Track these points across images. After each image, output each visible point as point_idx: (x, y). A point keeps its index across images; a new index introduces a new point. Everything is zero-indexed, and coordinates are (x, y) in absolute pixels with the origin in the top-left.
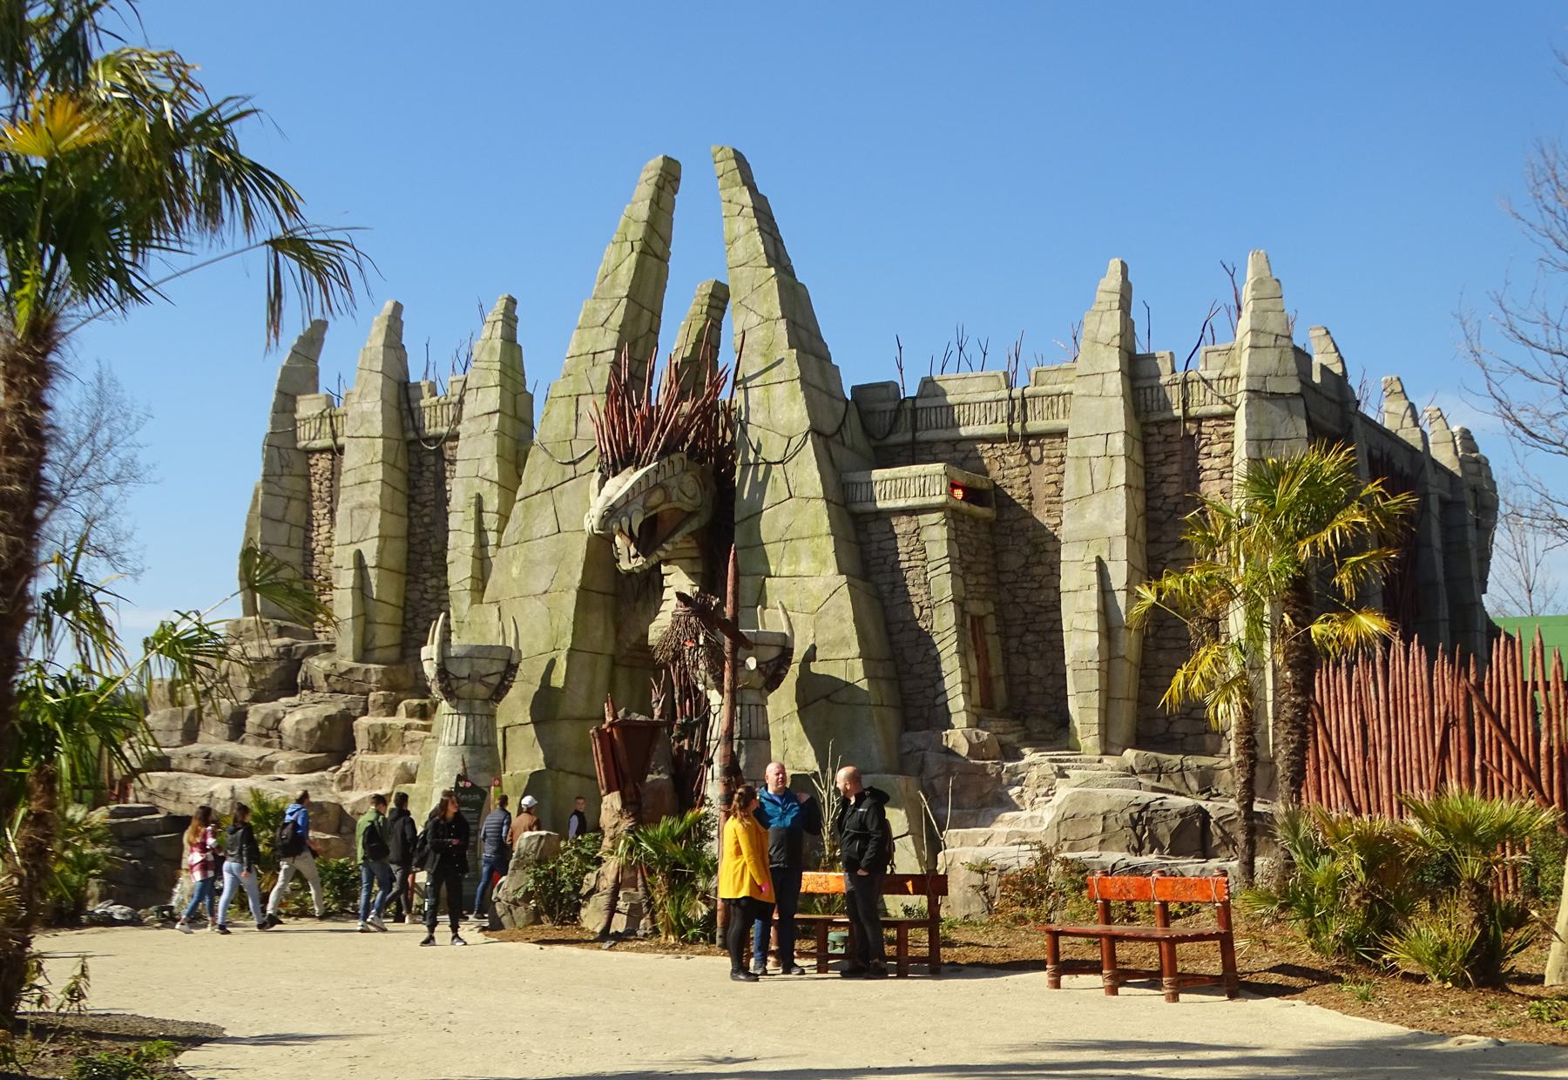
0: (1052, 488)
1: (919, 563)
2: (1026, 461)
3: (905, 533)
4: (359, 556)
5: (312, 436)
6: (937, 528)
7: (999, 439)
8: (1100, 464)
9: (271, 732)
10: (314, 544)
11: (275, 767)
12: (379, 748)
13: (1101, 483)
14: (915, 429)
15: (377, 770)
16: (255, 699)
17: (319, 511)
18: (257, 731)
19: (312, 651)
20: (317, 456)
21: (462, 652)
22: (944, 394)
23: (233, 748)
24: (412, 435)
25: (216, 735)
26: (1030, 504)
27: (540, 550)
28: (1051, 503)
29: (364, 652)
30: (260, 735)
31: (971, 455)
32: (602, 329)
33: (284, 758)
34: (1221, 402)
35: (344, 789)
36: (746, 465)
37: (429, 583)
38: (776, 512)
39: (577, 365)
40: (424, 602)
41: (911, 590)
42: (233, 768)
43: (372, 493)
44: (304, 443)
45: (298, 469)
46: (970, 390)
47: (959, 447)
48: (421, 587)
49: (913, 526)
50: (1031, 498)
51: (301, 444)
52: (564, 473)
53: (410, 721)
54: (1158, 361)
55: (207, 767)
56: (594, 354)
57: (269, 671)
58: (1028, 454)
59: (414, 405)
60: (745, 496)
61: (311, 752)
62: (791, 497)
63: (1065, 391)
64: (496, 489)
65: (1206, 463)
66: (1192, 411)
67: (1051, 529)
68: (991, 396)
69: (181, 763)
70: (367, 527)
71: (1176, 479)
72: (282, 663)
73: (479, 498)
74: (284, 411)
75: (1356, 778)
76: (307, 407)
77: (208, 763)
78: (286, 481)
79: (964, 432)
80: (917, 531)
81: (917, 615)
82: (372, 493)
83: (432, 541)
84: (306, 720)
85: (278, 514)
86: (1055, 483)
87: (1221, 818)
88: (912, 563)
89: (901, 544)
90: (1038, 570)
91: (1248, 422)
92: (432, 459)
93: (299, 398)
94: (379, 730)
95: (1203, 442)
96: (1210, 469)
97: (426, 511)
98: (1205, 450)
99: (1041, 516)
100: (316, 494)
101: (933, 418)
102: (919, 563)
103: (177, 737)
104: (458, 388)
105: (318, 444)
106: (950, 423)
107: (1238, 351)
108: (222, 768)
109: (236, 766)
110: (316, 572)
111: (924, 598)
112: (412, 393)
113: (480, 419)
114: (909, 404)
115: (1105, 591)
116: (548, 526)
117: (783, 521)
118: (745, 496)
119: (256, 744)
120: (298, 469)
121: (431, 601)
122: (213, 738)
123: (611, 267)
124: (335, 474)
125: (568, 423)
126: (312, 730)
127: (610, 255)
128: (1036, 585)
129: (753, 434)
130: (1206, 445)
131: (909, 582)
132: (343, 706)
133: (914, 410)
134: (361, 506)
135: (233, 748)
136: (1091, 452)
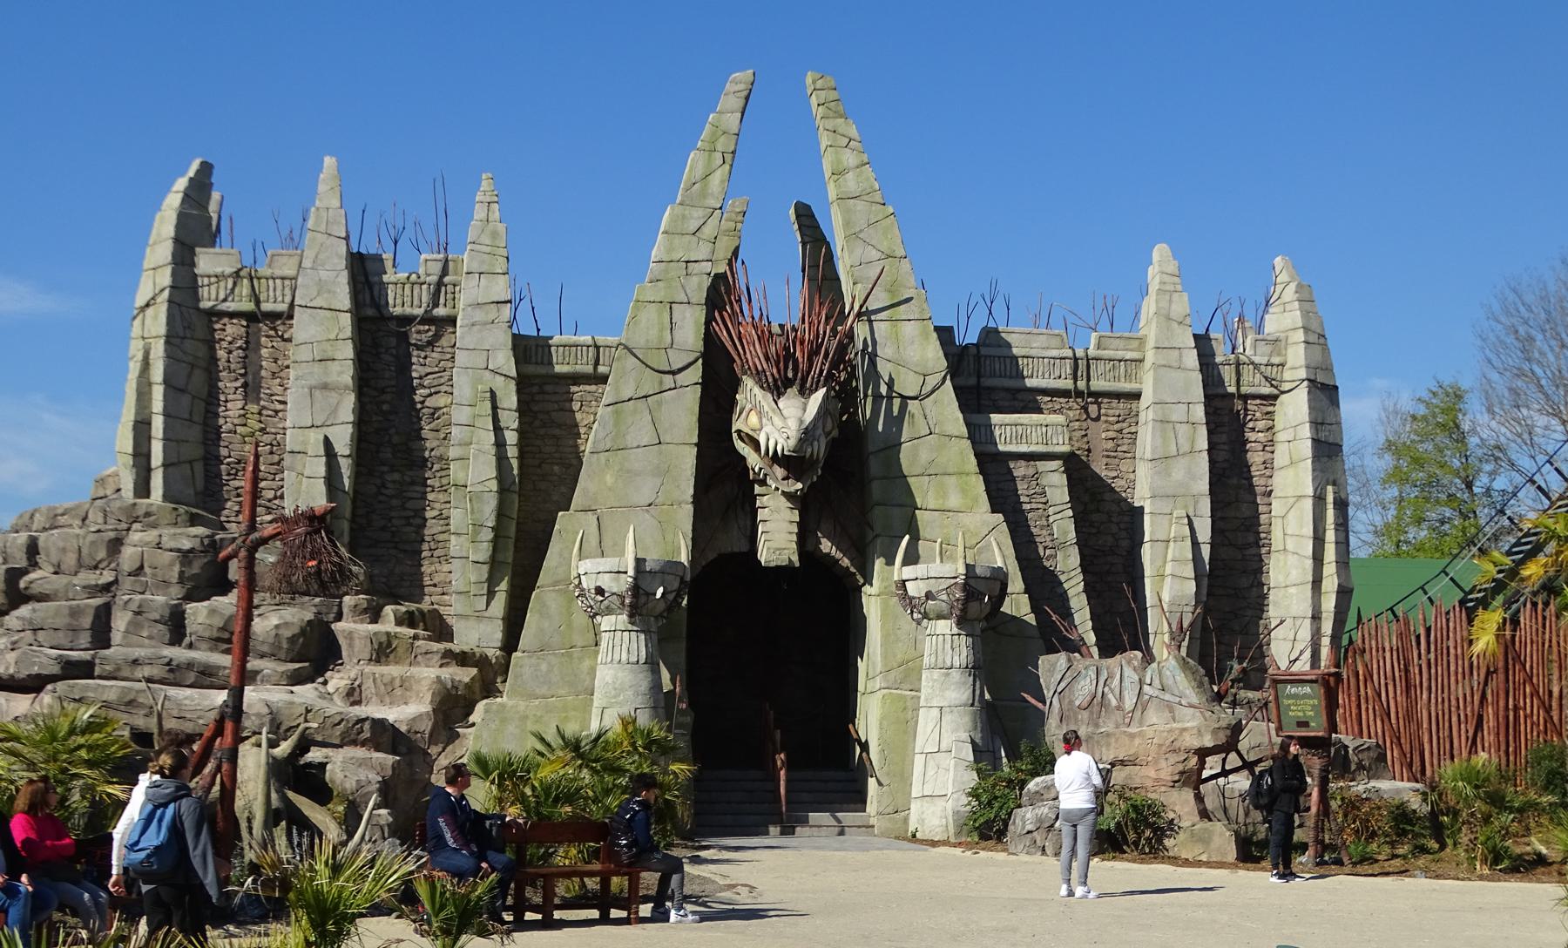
0: (1110, 444)
1: (1040, 506)
2: (1085, 416)
3: (1024, 477)
4: (327, 443)
5: (222, 296)
6: (1056, 475)
7: (1065, 393)
10: (221, 421)
11: (259, 677)
12: (383, 659)
13: (1185, 448)
14: (979, 377)
15: (397, 683)
16: (190, 597)
18: (215, 634)
20: (226, 320)
22: (1009, 346)
23: (179, 654)
24: (370, 312)
25: (150, 637)
26: (1088, 456)
27: (638, 460)
28: (1108, 457)
30: (218, 640)
31: (1031, 405)
32: (695, 239)
34: (1268, 384)
35: (353, 704)
36: (877, 397)
37: (389, 477)
38: (913, 445)
39: (666, 271)
40: (381, 498)
41: (1034, 530)
43: (340, 373)
44: (211, 304)
46: (1034, 345)
47: (1019, 396)
48: (378, 482)
49: (1031, 471)
50: (1089, 450)
51: (206, 304)
52: (661, 383)
53: (398, 629)
54: (1213, 342)
55: (171, 676)
56: (687, 262)
57: (196, 568)
58: (1085, 409)
60: (880, 428)
61: (292, 661)
62: (931, 433)
63: (1127, 358)
64: (512, 386)
65: (1251, 436)
66: (1244, 390)
67: (1109, 481)
68: (1055, 353)
69: (119, 669)
70: (335, 411)
71: (1226, 447)
73: (492, 392)
74: (183, 264)
75: (1397, 713)
76: (207, 262)
77: (171, 671)
78: (189, 345)
79: (1029, 383)
80: (1037, 475)
81: (1042, 554)
82: (340, 373)
83: (392, 431)
86: (1113, 439)
87: (1357, 748)
88: (1034, 506)
89: (1021, 487)
90: (1095, 517)
91: (1310, 408)
92: (393, 341)
93: (198, 250)
94: (384, 639)
95: (1249, 417)
96: (1255, 442)
97: (388, 397)
98: (1251, 425)
100: (222, 364)
101: (997, 366)
102: (1040, 506)
103: (85, 639)
104: (436, 268)
105: (231, 306)
106: (1014, 373)
107: (1283, 343)
108: (191, 677)
109: (211, 675)
110: (224, 452)
111: (1048, 538)
112: (370, 266)
113: (488, 306)
114: (973, 351)
115: (1195, 544)
116: (647, 437)
117: (924, 456)
118: (880, 428)
119: (211, 650)
121: (391, 497)
122: (147, 641)
123: (699, 173)
124: (250, 346)
125: (661, 330)
126: (294, 636)
128: (1094, 531)
129: (884, 369)
130: (1251, 420)
131: (1031, 523)
132: (314, 610)
133: (978, 357)
134: (325, 387)
135: (179, 654)
136: (1174, 418)
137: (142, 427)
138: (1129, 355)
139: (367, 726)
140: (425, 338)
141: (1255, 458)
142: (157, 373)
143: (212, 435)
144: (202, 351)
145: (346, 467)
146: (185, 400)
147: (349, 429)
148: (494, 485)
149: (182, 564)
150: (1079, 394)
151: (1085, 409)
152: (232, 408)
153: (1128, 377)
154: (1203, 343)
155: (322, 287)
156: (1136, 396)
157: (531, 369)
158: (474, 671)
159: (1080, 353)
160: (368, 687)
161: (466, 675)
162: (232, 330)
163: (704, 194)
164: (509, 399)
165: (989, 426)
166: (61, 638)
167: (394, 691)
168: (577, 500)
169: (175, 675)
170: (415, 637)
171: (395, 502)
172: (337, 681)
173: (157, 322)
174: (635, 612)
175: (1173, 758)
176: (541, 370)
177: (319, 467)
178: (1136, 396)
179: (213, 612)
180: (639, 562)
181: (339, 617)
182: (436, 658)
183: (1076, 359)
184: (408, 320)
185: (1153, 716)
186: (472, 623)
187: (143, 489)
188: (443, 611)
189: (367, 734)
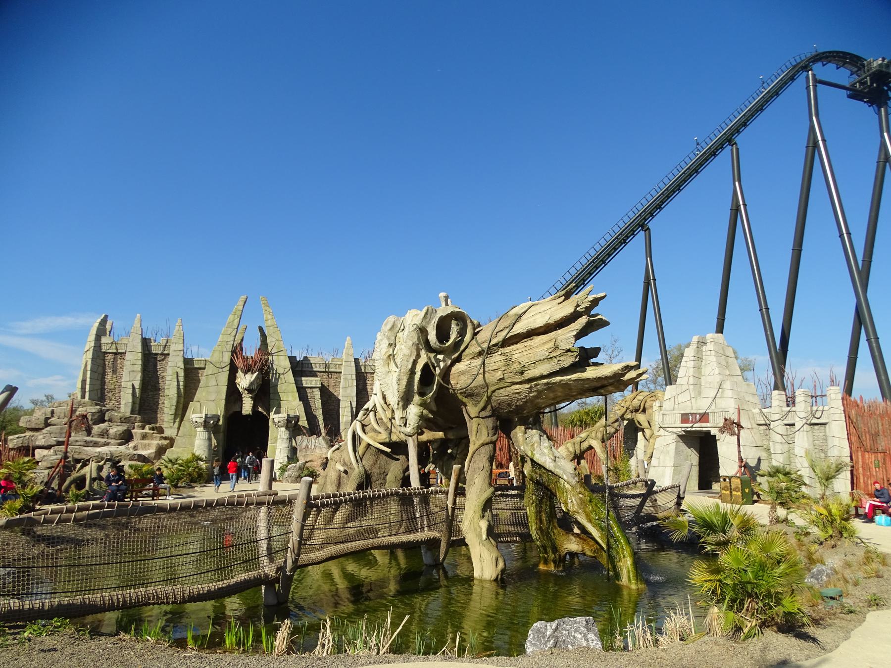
4: (133, 385)
7: (323, 372)
8: (350, 381)
9: (104, 434)
16: (95, 424)
17: (108, 370)
18: (99, 433)
19: (108, 410)
21: (210, 416)
23: (89, 439)
24: (147, 352)
29: (132, 412)
33: (112, 441)
36: (273, 374)
42: (96, 445)
45: (101, 358)
51: (103, 350)
57: (96, 417)
58: (328, 376)
59: (148, 344)
64: (183, 371)
66: (366, 371)
70: (135, 377)
72: (100, 414)
73: (177, 373)
76: (104, 340)
79: (314, 369)
84: (119, 431)
85: (95, 370)
89: (309, 395)
90: (329, 401)
99: (331, 389)
100: (107, 365)
104: (165, 341)
110: (106, 387)
115: (352, 408)
116: (214, 383)
117: (284, 388)
120: (101, 358)
124: (115, 360)
127: (231, 317)
129: (275, 367)
133: (302, 363)
134: (133, 371)
135: (89, 439)
137: (84, 382)
138: (339, 363)
139: (136, 456)
140: (161, 358)
141: (369, 387)
142: (89, 368)
143: (103, 383)
144: (101, 362)
145: (137, 391)
146: (96, 374)
147: (139, 381)
148: (176, 395)
149: (92, 416)
150: (326, 372)
151: (328, 376)
152: (109, 376)
153: (339, 368)
154: (356, 361)
155: (134, 346)
156: (341, 373)
157: (189, 366)
158: (168, 441)
159: (327, 362)
160: (140, 446)
161: (166, 442)
162: (110, 357)
163: (232, 325)
164: (182, 374)
165: (301, 380)
166: (57, 435)
167: (145, 447)
168: (195, 399)
169: (87, 444)
170: (153, 433)
171: (151, 399)
172: (131, 444)
173: (90, 355)
174: (205, 427)
175: (321, 460)
176: (192, 367)
177: (130, 391)
178: (341, 373)
179: (99, 428)
180: (206, 415)
181: (134, 428)
182: (158, 438)
183: (326, 364)
184: (157, 354)
185: (317, 450)
186: (169, 429)
187: (83, 397)
188: (162, 426)
189: (136, 458)
